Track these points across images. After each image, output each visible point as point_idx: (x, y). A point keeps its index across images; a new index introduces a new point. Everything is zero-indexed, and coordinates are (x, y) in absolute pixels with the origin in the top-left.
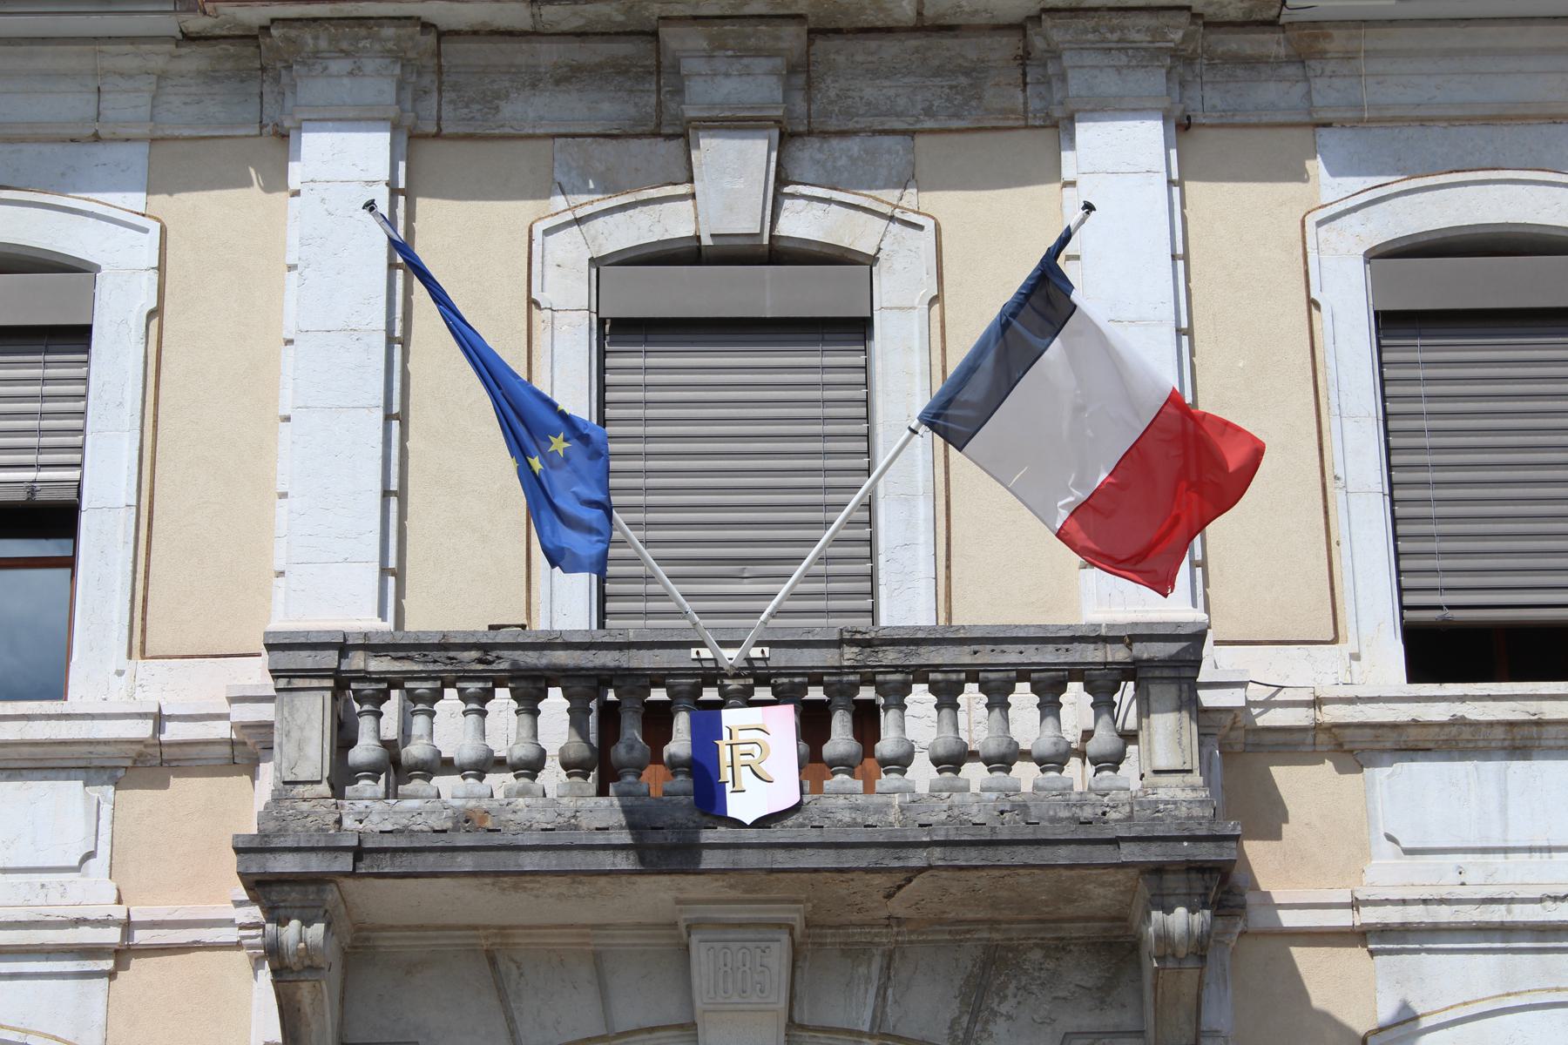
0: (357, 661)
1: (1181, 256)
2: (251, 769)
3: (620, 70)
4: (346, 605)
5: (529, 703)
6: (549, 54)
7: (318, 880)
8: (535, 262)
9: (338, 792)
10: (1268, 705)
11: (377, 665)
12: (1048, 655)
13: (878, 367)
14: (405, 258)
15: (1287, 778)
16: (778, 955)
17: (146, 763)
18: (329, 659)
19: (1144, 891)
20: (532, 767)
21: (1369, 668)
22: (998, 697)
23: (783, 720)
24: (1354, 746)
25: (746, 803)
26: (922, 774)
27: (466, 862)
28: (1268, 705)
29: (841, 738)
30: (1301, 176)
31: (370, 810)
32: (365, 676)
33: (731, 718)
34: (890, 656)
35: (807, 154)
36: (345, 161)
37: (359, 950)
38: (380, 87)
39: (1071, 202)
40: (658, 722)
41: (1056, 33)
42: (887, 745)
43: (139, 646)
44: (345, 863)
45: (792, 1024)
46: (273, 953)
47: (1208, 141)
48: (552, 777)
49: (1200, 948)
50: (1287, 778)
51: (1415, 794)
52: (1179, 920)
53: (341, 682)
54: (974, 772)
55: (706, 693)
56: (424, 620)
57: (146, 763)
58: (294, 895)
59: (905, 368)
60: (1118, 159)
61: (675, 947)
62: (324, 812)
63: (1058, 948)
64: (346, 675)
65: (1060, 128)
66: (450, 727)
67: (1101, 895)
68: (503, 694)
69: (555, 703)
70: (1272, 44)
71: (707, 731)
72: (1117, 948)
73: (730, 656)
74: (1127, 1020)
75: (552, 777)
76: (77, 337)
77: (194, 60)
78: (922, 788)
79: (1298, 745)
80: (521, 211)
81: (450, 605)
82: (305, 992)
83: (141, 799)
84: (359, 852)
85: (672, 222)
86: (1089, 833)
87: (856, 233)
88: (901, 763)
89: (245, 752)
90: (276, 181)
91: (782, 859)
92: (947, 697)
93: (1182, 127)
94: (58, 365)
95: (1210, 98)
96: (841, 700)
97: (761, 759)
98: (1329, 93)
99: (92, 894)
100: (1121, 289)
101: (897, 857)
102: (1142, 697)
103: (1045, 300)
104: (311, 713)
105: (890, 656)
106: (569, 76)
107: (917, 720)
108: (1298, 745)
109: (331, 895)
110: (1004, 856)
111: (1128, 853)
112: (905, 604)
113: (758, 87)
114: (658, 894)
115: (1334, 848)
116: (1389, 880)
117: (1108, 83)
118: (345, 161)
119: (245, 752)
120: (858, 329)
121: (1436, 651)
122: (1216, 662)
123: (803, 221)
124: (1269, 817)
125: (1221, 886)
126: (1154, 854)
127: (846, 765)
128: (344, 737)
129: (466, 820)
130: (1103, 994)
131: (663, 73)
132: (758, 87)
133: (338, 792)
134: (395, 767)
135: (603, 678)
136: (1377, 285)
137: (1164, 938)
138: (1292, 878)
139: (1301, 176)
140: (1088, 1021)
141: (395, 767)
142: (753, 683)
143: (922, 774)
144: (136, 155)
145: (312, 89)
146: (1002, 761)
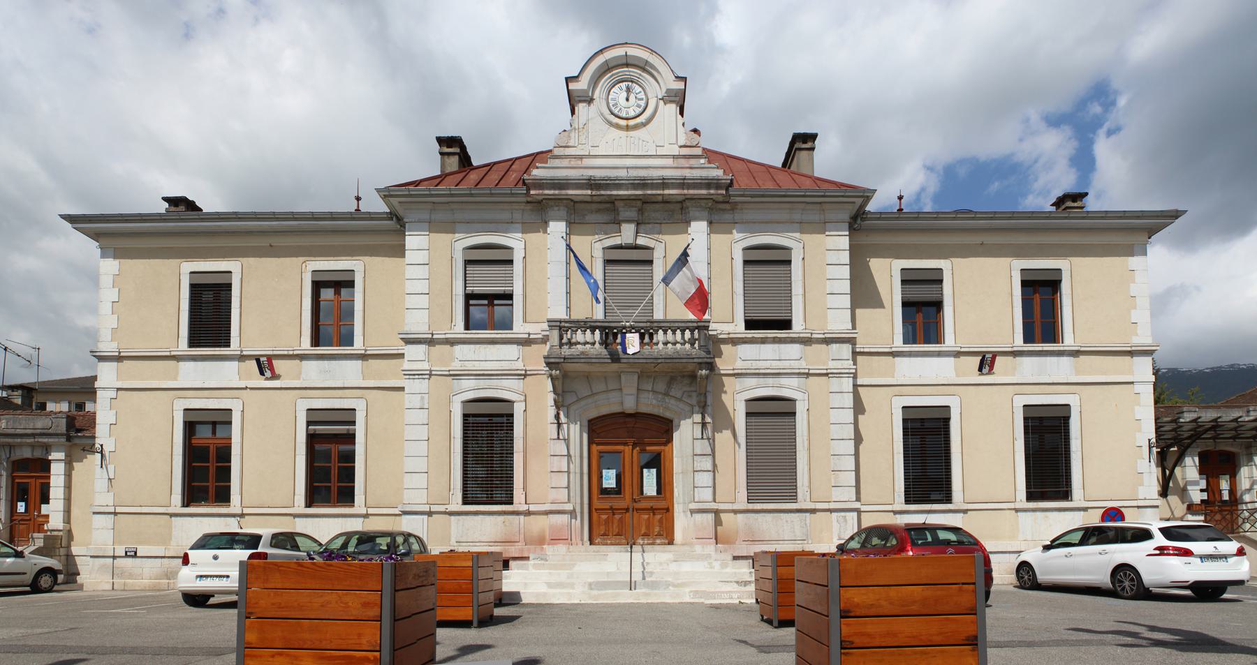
1: (709, 249)
2: (545, 343)
3: (607, 210)
4: (561, 314)
6: (594, 206)
8: (592, 247)
14: (569, 247)
15: (723, 347)
16: (636, 377)
17: (526, 342)
20: (594, 344)
21: (739, 328)
22: (674, 332)
24: (735, 342)
29: (647, 339)
30: (731, 233)
35: (642, 227)
36: (557, 228)
37: (565, 375)
38: (563, 213)
39: (690, 238)
40: (615, 336)
41: (688, 203)
43: (525, 321)
47: (715, 226)
48: (597, 345)
50: (723, 347)
51: (745, 351)
52: (704, 372)
53: (560, 328)
55: (623, 331)
56: (574, 317)
57: (526, 342)
59: (659, 271)
60: (698, 229)
63: (683, 376)
65: (688, 223)
66: (579, 336)
67: (690, 367)
70: (727, 206)
72: (693, 377)
75: (597, 345)
76: (511, 262)
77: (529, 207)
79: (725, 341)
80: (590, 238)
81: (579, 314)
83: (527, 348)
85: (617, 241)
86: (689, 357)
87: (651, 243)
89: (545, 340)
90: (545, 232)
92: (665, 332)
93: (710, 223)
94: (507, 267)
95: (716, 217)
98: (737, 217)
99: (519, 365)
100: (698, 265)
101: (656, 361)
103: (684, 258)
104: (556, 333)
106: (598, 211)
108: (725, 341)
113: (632, 213)
114: (615, 366)
115: (731, 359)
116: (739, 365)
117: (697, 214)
118: (557, 228)
119: (545, 340)
120: (650, 262)
121: (751, 324)
122: (712, 326)
123: (641, 241)
124: (720, 354)
125: (711, 366)
131: (615, 211)
132: (632, 213)
134: (570, 343)
135: (606, 328)
136: (744, 255)
138: (723, 365)
139: (731, 233)
141: (570, 343)
142: (632, 329)
144: (519, 226)
145: (551, 213)
146: (674, 344)
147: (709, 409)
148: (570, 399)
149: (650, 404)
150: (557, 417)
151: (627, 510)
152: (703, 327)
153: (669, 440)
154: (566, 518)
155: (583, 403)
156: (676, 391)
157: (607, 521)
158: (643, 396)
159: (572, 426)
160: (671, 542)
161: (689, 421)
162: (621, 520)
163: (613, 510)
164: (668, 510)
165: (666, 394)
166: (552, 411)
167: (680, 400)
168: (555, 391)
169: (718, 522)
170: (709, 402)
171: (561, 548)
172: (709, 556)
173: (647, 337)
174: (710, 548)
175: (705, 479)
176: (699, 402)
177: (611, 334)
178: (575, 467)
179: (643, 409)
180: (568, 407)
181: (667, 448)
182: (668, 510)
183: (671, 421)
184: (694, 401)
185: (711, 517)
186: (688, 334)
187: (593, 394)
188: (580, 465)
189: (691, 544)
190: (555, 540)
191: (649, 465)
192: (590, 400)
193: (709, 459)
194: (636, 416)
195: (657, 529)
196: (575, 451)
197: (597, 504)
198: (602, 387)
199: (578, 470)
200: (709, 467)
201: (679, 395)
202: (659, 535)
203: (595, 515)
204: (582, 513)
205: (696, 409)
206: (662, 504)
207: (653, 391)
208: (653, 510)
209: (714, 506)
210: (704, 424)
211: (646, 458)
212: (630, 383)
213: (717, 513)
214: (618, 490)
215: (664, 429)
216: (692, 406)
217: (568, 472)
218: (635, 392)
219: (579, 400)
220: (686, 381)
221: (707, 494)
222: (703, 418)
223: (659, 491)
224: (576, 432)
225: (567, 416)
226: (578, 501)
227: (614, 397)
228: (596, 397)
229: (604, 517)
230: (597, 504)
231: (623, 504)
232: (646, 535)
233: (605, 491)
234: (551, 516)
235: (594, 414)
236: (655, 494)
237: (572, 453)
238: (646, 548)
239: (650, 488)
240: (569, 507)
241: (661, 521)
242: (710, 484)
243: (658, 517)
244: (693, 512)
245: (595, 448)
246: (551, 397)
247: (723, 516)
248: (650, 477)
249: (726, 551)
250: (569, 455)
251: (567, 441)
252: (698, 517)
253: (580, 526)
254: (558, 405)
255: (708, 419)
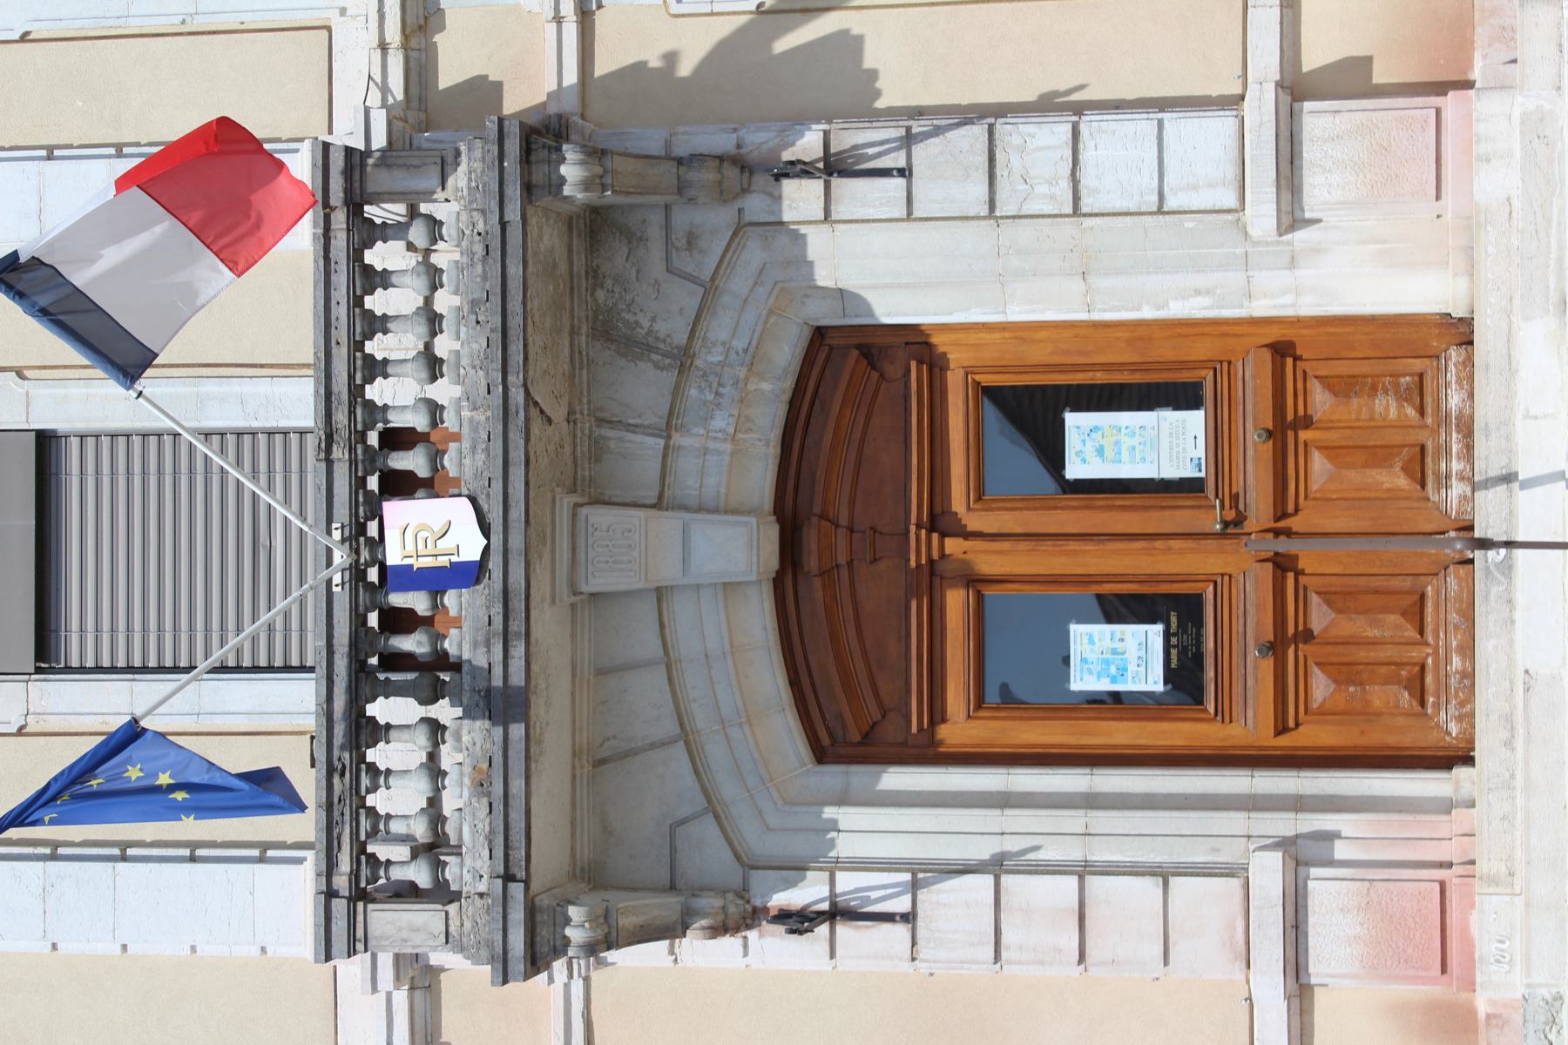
0: (341, 883)
2: (434, 972)
5: (378, 732)
7: (531, 911)
9: (455, 897)
10: (385, 89)
11: (345, 865)
12: (340, 280)
13: (81, 426)
15: (450, 73)
16: (599, 517)
18: (340, 906)
19: (546, 201)
20: (436, 729)
23: (395, 510)
25: (470, 545)
26: (444, 391)
27: (517, 785)
28: (385, 89)
29: (411, 461)
31: (471, 868)
32: (355, 875)
33: (393, 557)
34: (341, 417)
37: (592, 876)
40: (399, 621)
42: (420, 422)
44: (517, 889)
45: (658, 505)
46: (592, 949)
49: (595, 154)
50: (450, 73)
52: (572, 171)
53: (360, 895)
54: (444, 346)
55: (372, 579)
58: (544, 933)
59: (83, 401)
61: (592, 605)
62: (472, 907)
63: (594, 274)
64: (354, 892)
66: (401, 801)
67: (549, 238)
68: (371, 755)
69: (379, 709)
71: (409, 578)
72: (594, 225)
73: (340, 557)
74: (656, 218)
78: (457, 391)
79: (420, 67)
82: (627, 921)
84: (508, 878)
88: (435, 410)
89: (420, 977)
91: (517, 512)
92: (376, 368)
96: (379, 461)
97: (430, 530)
101: (516, 413)
102: (376, 199)
105: (341, 417)
107: (397, 395)
108: (420, 67)
109: (544, 901)
110: (515, 321)
111: (513, 213)
112: (294, 404)
119: (420, 977)
122: (346, 134)
124: (483, 92)
125: (542, 136)
126: (514, 191)
127: (436, 457)
128: (408, 892)
129: (481, 786)
130: (634, 238)
133: (455, 897)
134: (434, 848)
135: (359, 669)
137: (586, 185)
138: (536, 77)
140: (656, 252)
141: (434, 848)
143: (444, 391)
146: (434, 322)
147: (757, 140)
148: (708, 854)
149: (734, 445)
150: (798, 921)
151: (1282, 565)
152: (353, 181)
153: (915, 343)
154: (1323, 890)
155: (728, 790)
156: (666, 311)
157: (1345, 673)
158: (691, 477)
159: (845, 847)
160: (1460, 331)
161: (818, 243)
162: (1337, 598)
163: (1284, 641)
164: (1282, 351)
165: (683, 360)
166: (771, 948)
167: (710, 290)
168: (671, 930)
169: (1350, 80)
170: (722, 142)
171: (1489, 921)
172: (1538, 129)
173: (403, 461)
174: (1490, 117)
175: (1118, 155)
176: (723, 195)
177: (381, 645)
178: (1058, 835)
179: (760, 479)
180: (748, 864)
181: (957, 357)
182: (1284, 347)
183: (820, 334)
184: (715, 219)
185: (1318, 119)
186: (379, 256)
187: (686, 736)
188: (1046, 813)
189: (1471, 225)
190: (1447, 952)
191: (1052, 452)
192: (715, 754)
193: (1012, 133)
194: (791, 517)
195: (1388, 407)
196: (973, 833)
197: (1252, 724)
198: (647, 690)
199: (1074, 820)
200: (1055, 132)
201: (686, 298)
202: (1418, 393)
203: (1311, 736)
204: (1299, 804)
205: (754, 206)
206: (1254, 377)
207: (669, 426)
208: (1285, 428)
209: (1261, 106)
210: (835, 166)
211: (1013, 457)
212: (629, 548)
213: (1297, 89)
214: (1176, 609)
215: (858, 374)
216: (740, 228)
217: (1084, 870)
218: (667, 525)
219: (714, 808)
220: (616, 258)
221: (1200, 143)
222: (801, 169)
223: (1182, 396)
224: (882, 825)
225: (796, 869)
226: (1235, 821)
227: (698, 628)
228: (701, 719)
229: (1321, 687)
230: (1252, 724)
231: (1254, 587)
232: (1419, 465)
233: (1185, 675)
234: (1317, 970)
235: (782, 732)
236: (1195, 420)
237: (983, 850)
238: (1488, 459)
239: (1166, 443)
240: (1268, 872)
241: (1342, 387)
242: (1141, 126)
243: (1320, 401)
244: (1292, 218)
245: (958, 730)
246: (704, 954)
247: (1312, 59)
248: (1099, 444)
249: (1507, 35)
250: (997, 866)
251: (922, 874)
252: (1318, 189)
253: (1370, 816)
254: (740, 918)
255: (809, 144)
